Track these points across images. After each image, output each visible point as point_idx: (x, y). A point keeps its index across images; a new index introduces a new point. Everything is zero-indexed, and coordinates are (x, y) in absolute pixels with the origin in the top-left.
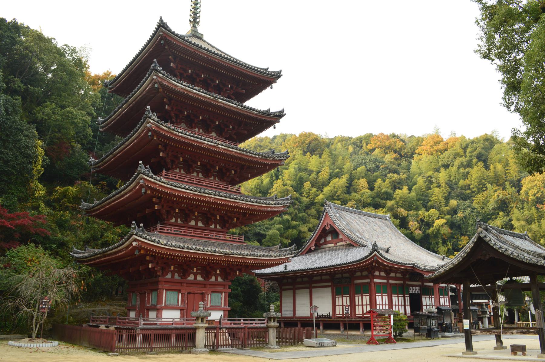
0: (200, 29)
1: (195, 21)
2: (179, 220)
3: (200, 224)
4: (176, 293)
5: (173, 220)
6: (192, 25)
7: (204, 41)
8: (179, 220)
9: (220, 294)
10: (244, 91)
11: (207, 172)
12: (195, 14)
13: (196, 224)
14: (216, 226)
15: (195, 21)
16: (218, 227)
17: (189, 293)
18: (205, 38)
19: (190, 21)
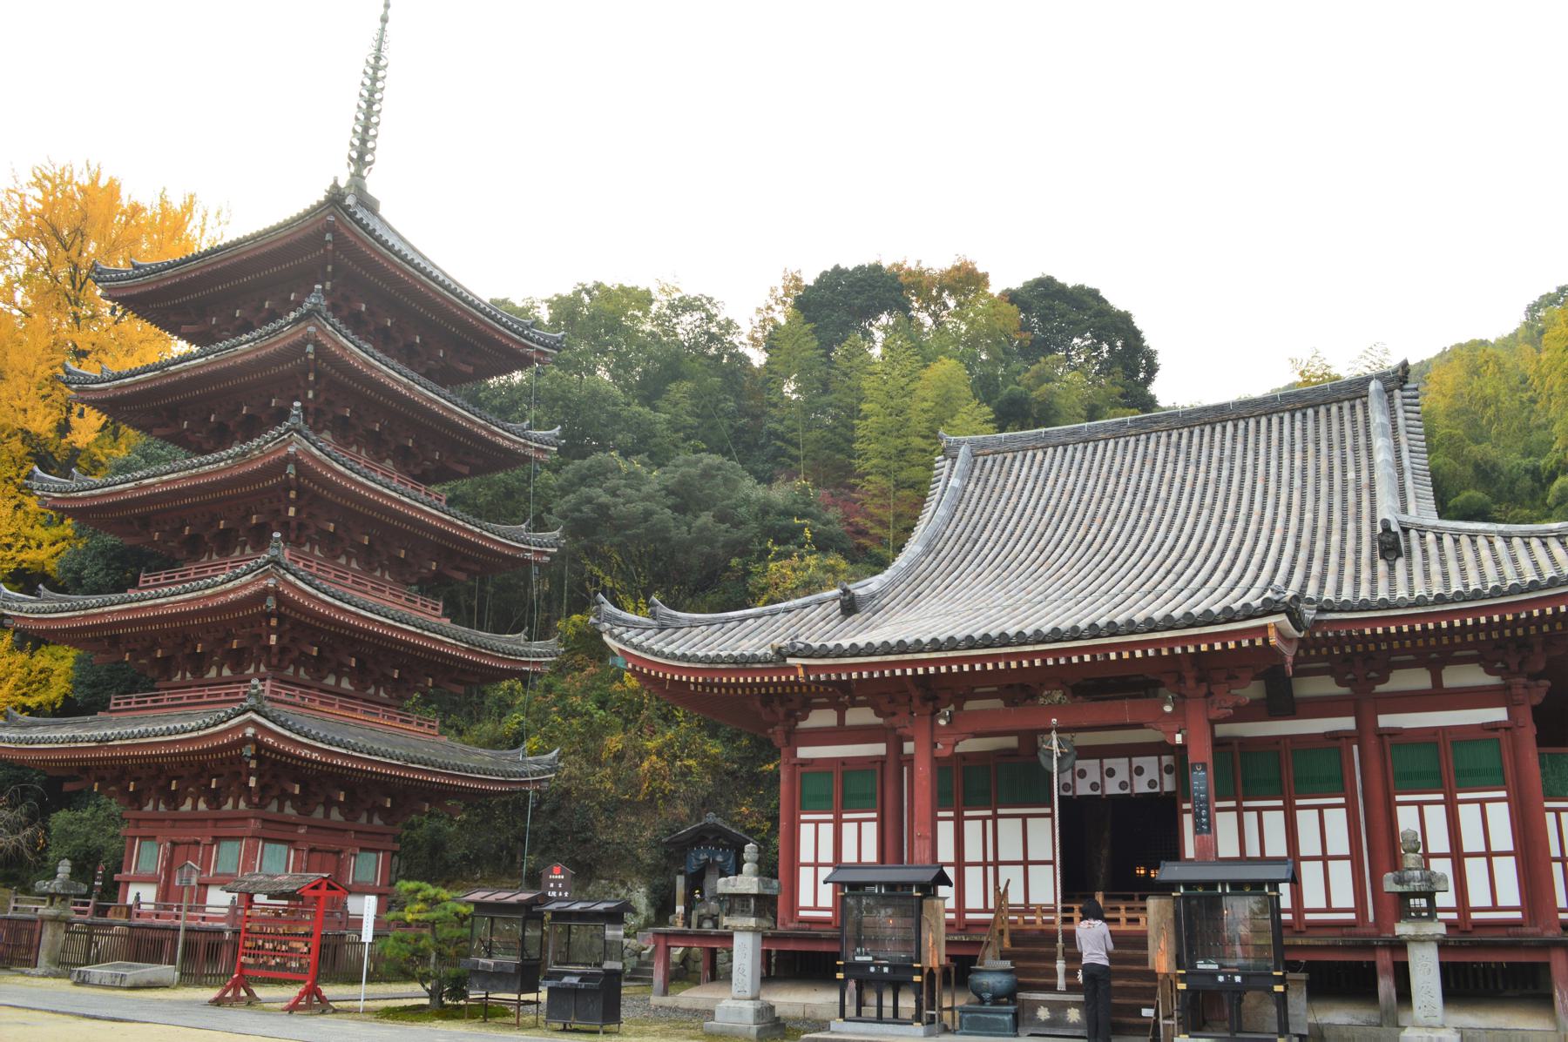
0: (373, 187)
1: (361, 159)
2: (302, 672)
3: (346, 684)
4: (283, 848)
5: (291, 669)
6: (353, 169)
7: (382, 220)
8: (302, 672)
9: (373, 856)
10: (470, 369)
11: (370, 559)
12: (364, 142)
13: (338, 682)
14: (377, 692)
15: (361, 159)
16: (382, 693)
17: (312, 850)
18: (382, 212)
19: (351, 159)
